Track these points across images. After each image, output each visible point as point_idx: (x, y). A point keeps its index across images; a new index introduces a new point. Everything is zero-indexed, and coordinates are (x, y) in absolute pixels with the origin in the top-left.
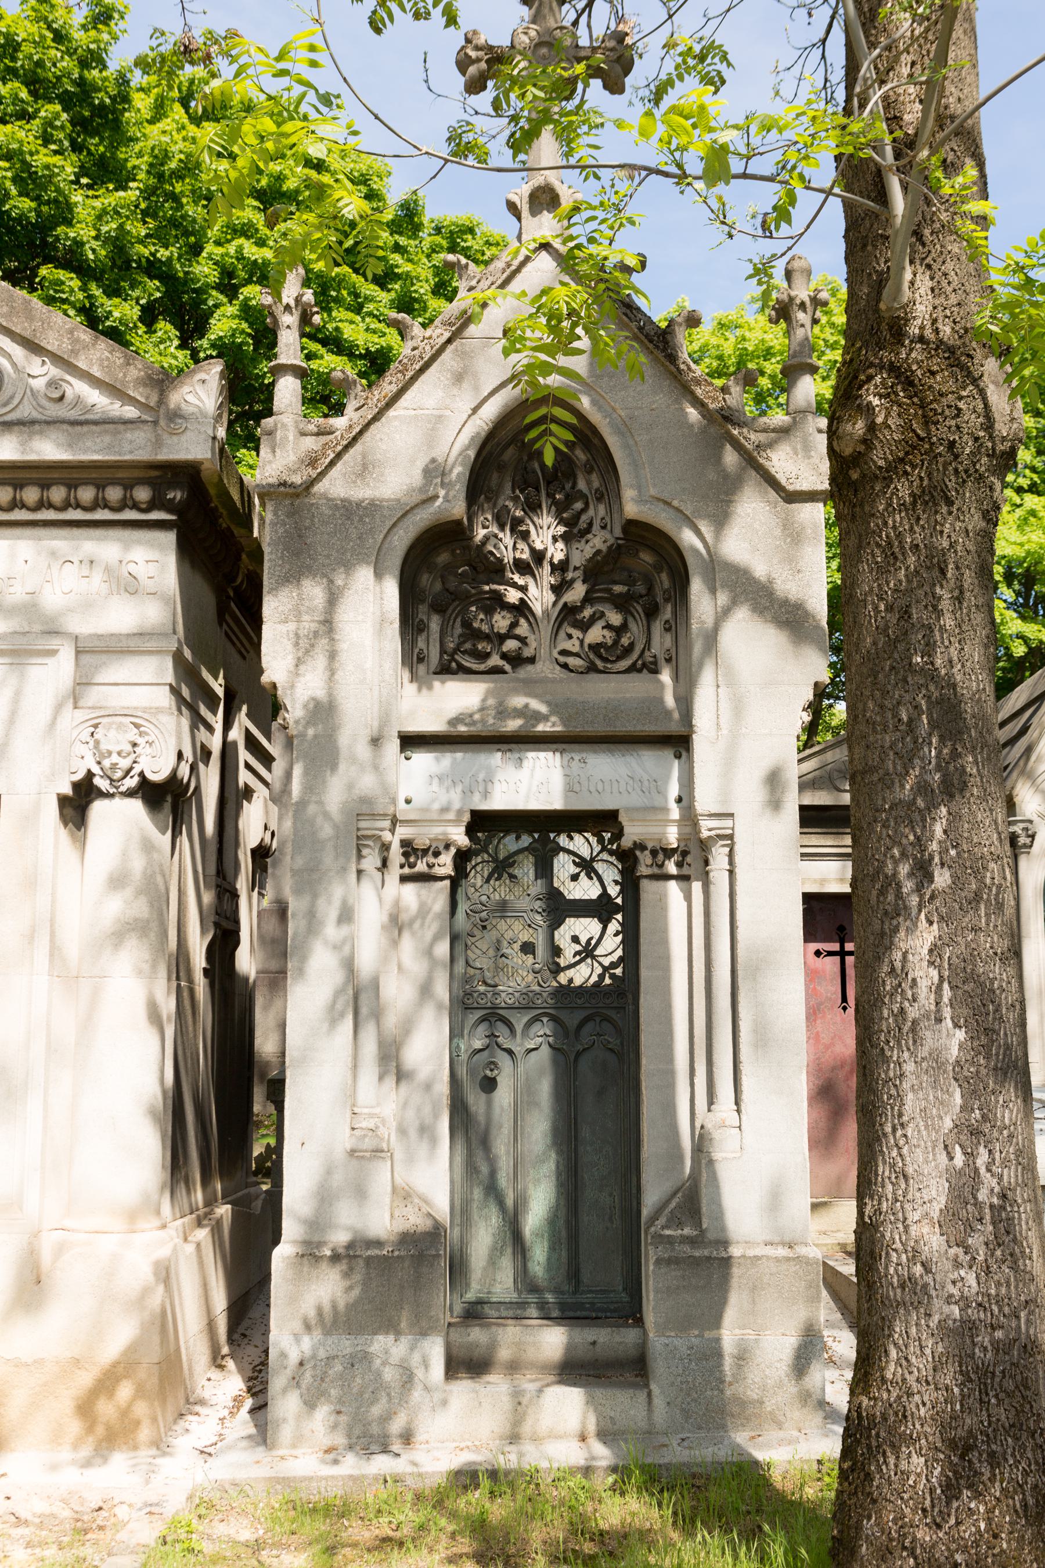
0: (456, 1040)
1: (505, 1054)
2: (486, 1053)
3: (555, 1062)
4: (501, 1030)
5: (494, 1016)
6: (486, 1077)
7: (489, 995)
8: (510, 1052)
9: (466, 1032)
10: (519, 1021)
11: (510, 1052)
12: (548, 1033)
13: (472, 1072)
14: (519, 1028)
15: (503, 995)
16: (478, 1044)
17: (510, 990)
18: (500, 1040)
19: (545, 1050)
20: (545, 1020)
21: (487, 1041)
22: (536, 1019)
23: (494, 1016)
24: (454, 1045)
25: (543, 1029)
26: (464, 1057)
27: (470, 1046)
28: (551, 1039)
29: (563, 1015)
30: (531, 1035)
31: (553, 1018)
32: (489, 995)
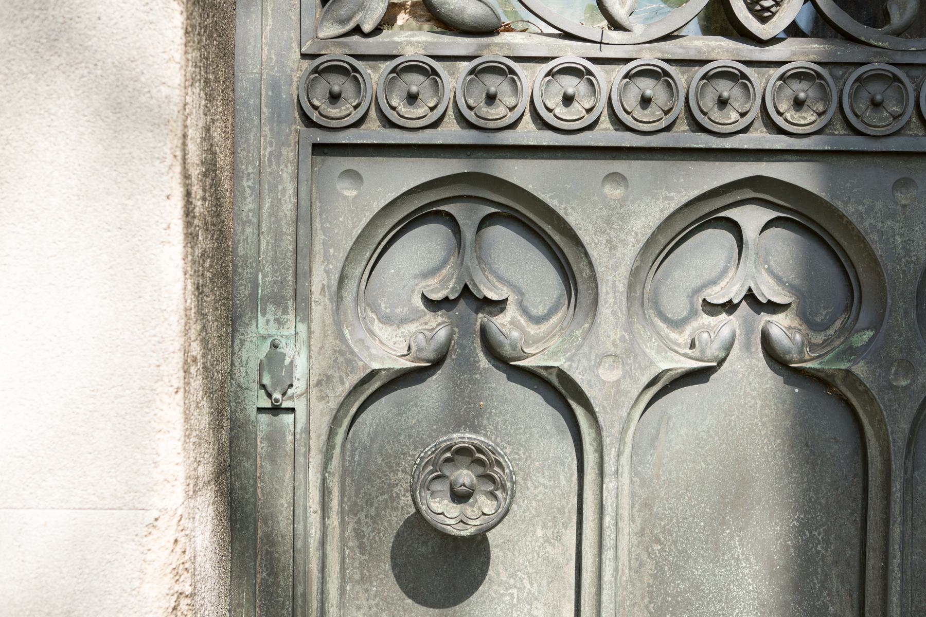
0: (263, 326)
1: (531, 400)
2: (431, 391)
3: (805, 448)
4: (514, 267)
5: (476, 192)
6: (419, 525)
7: (454, 79)
8: (561, 391)
9: (321, 277)
10: (616, 215)
11: (561, 391)
12: (769, 291)
13: (361, 487)
14: (613, 260)
15: (531, 78)
16: (389, 346)
17: (571, 53)
18: (507, 325)
19: (749, 384)
20: (752, 219)
21: (438, 328)
22: (706, 215)
23: (476, 192)
24: (253, 352)
25: (765, 259)
26: (311, 414)
27: (344, 355)
28: (781, 327)
29: (861, 200)
30: (677, 305)
31: (799, 214)
32: (454, 79)
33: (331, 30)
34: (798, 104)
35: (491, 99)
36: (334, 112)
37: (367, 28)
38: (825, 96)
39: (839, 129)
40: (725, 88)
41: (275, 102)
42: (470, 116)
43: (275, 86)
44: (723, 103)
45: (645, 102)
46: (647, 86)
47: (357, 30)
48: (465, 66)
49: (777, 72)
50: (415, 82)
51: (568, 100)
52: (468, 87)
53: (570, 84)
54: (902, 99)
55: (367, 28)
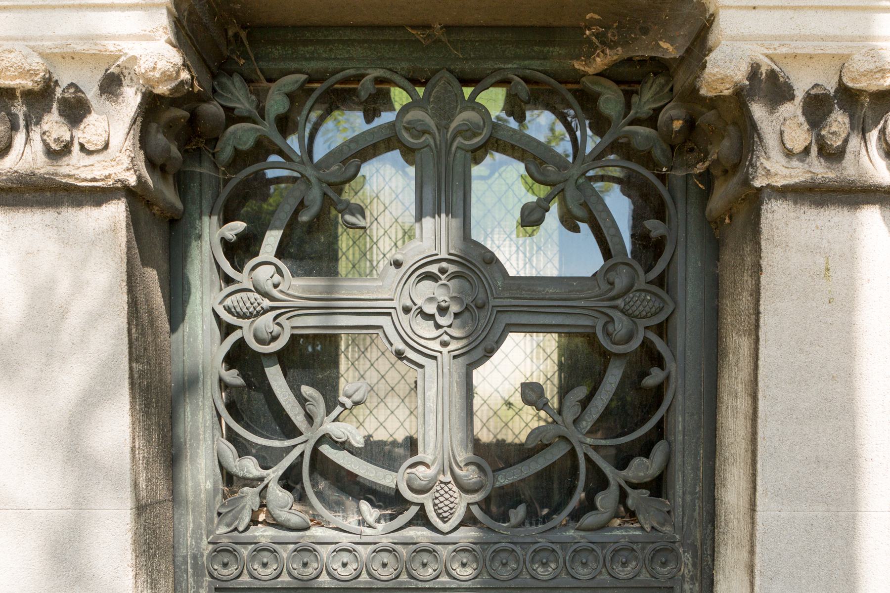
7: (285, 553)
15: (324, 552)
33: (223, 530)
34: (464, 565)
35: (305, 565)
36: (225, 572)
37: (241, 529)
38: (476, 559)
39: (486, 576)
40: (426, 558)
41: (195, 566)
42: (295, 573)
43: (195, 557)
44: (424, 565)
45: (384, 565)
46: (386, 557)
47: (236, 529)
48: (291, 547)
49: (451, 547)
50: (266, 557)
51: (344, 565)
52: (292, 559)
53: (345, 557)
54: (517, 561)
55: (241, 529)
